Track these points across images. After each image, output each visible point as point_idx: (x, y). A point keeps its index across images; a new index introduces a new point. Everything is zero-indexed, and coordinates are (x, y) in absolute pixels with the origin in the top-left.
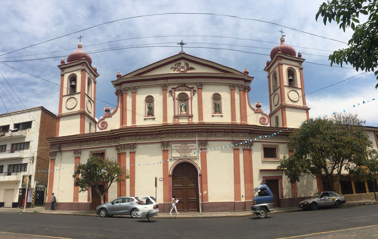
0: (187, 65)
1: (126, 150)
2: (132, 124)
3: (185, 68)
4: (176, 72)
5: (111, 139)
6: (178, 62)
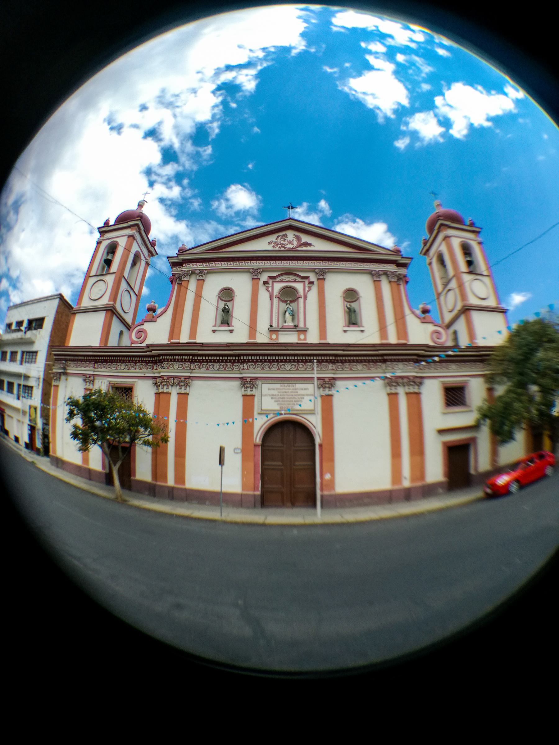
0: (298, 238)
1: (170, 387)
2: (190, 338)
3: (295, 243)
4: (277, 249)
5: (147, 363)
6: (284, 233)
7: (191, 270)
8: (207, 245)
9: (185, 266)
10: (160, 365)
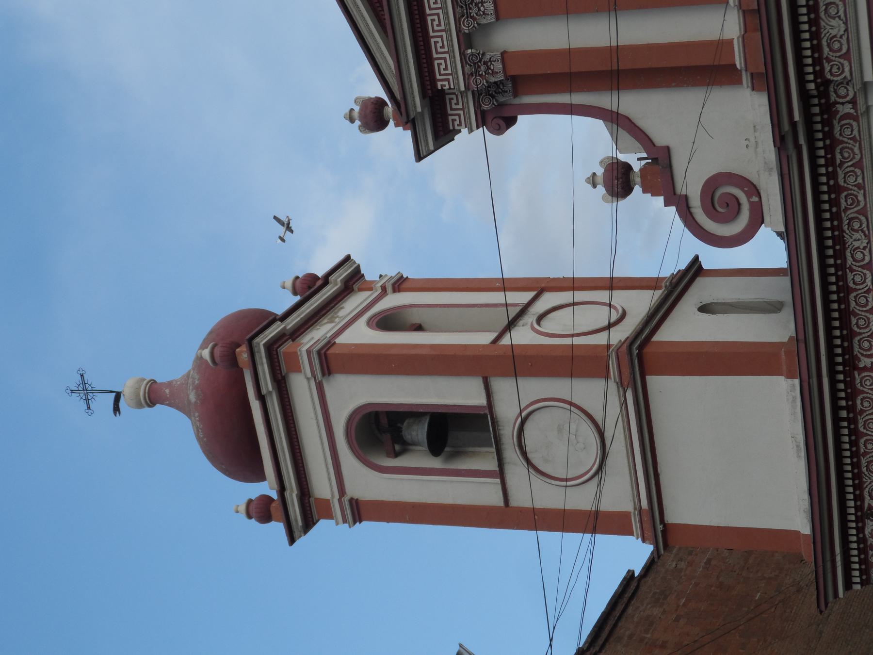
7: (462, 55)
8: (354, 13)
9: (446, 83)
10: (835, 92)
